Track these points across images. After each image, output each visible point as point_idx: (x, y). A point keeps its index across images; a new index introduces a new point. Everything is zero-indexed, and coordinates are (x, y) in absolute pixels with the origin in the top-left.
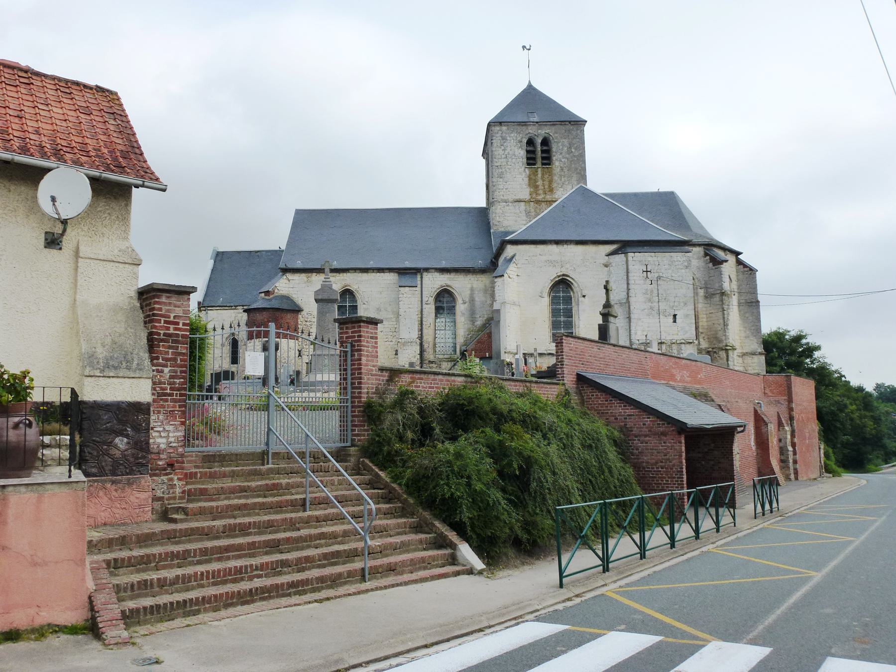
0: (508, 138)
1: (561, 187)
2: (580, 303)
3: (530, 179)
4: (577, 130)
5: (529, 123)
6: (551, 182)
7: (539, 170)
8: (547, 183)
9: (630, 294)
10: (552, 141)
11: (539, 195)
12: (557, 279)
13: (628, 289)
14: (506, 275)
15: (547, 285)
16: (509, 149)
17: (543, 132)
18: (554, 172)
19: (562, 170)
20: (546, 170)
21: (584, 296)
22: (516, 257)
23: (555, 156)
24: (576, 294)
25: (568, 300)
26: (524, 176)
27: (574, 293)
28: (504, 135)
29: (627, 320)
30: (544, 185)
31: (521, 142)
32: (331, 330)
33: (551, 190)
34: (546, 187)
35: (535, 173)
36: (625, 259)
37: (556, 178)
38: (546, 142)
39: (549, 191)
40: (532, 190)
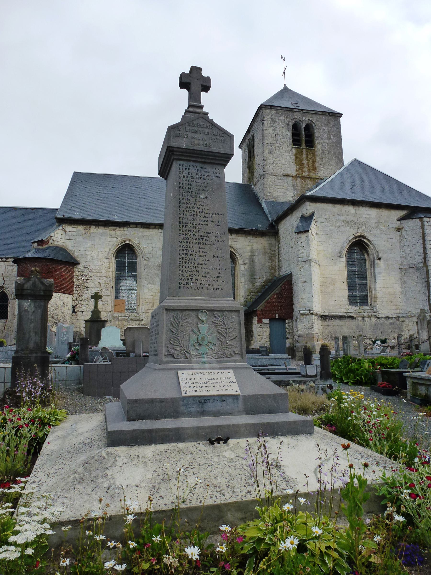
0: (277, 120)
1: (323, 167)
2: (376, 266)
3: (296, 158)
4: (335, 121)
5: (295, 110)
6: (314, 162)
7: (304, 151)
8: (310, 162)
9: (428, 258)
10: (315, 128)
11: (305, 172)
12: (354, 240)
13: (425, 253)
14: (310, 231)
15: (346, 245)
16: (278, 129)
17: (306, 119)
18: (316, 153)
19: (323, 152)
20: (310, 151)
21: (380, 259)
22: (315, 216)
23: (317, 140)
24: (371, 257)
25: (363, 263)
26: (291, 154)
27: (368, 254)
28: (273, 117)
29: (426, 284)
30: (308, 164)
31: (288, 125)
32: (213, 238)
33: (315, 169)
34: (310, 166)
35: (301, 153)
36: (420, 223)
37: (318, 159)
38: (309, 127)
39: (313, 170)
40: (298, 167)
